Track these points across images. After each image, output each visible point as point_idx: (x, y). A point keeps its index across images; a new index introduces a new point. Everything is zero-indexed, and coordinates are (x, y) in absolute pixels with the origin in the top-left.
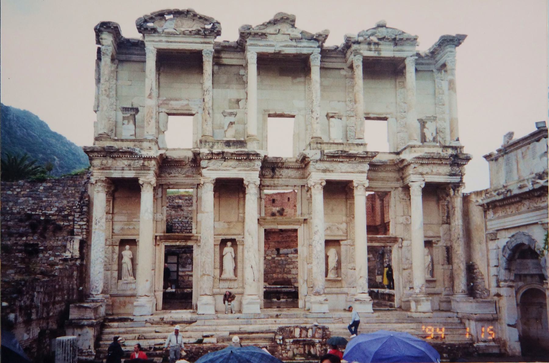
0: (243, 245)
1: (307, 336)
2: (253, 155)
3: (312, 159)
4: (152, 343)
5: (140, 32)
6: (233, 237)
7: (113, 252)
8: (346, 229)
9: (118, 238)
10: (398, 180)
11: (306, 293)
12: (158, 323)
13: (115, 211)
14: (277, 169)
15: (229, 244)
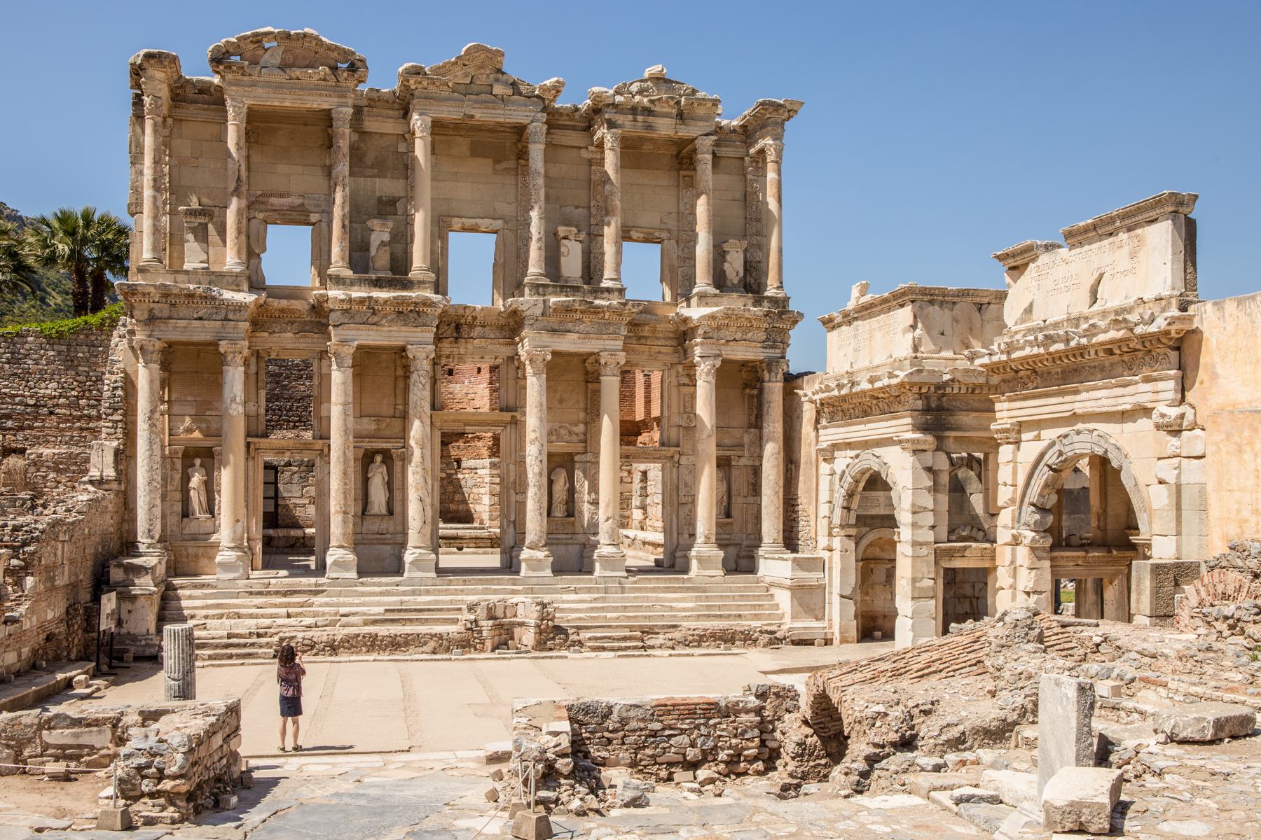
0: (403, 460)
1: (515, 616)
2: (424, 304)
3: (528, 313)
6: (384, 446)
7: (173, 469)
8: (585, 434)
9: (180, 448)
10: (676, 352)
11: (512, 544)
12: (260, 593)
13: (174, 397)
15: (379, 458)
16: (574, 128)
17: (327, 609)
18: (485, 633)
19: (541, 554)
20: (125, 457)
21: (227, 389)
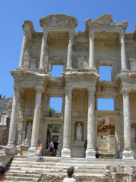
1: (123, 171)
4: (34, 169)
5: (42, 26)
6: (81, 120)
14: (104, 88)
15: (79, 124)
16: (131, 39)
17: (59, 167)
18: (113, 177)
19: (130, 152)
20: (8, 120)
21: (36, 99)
